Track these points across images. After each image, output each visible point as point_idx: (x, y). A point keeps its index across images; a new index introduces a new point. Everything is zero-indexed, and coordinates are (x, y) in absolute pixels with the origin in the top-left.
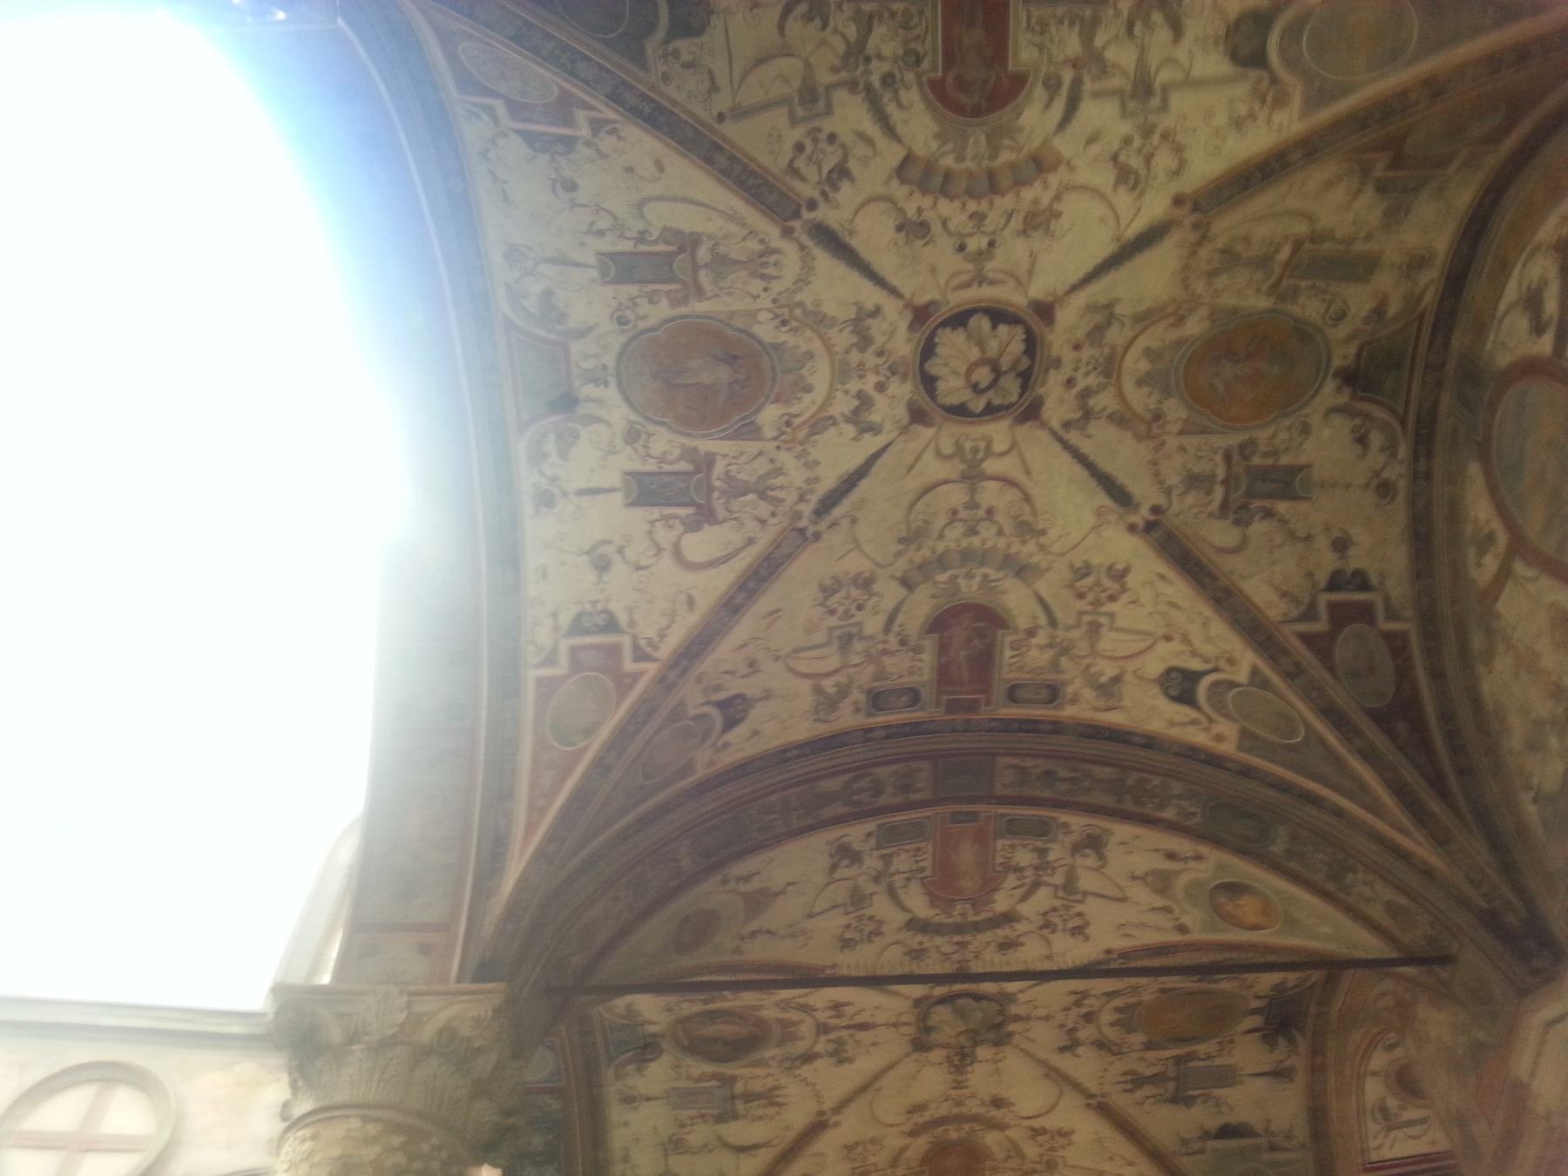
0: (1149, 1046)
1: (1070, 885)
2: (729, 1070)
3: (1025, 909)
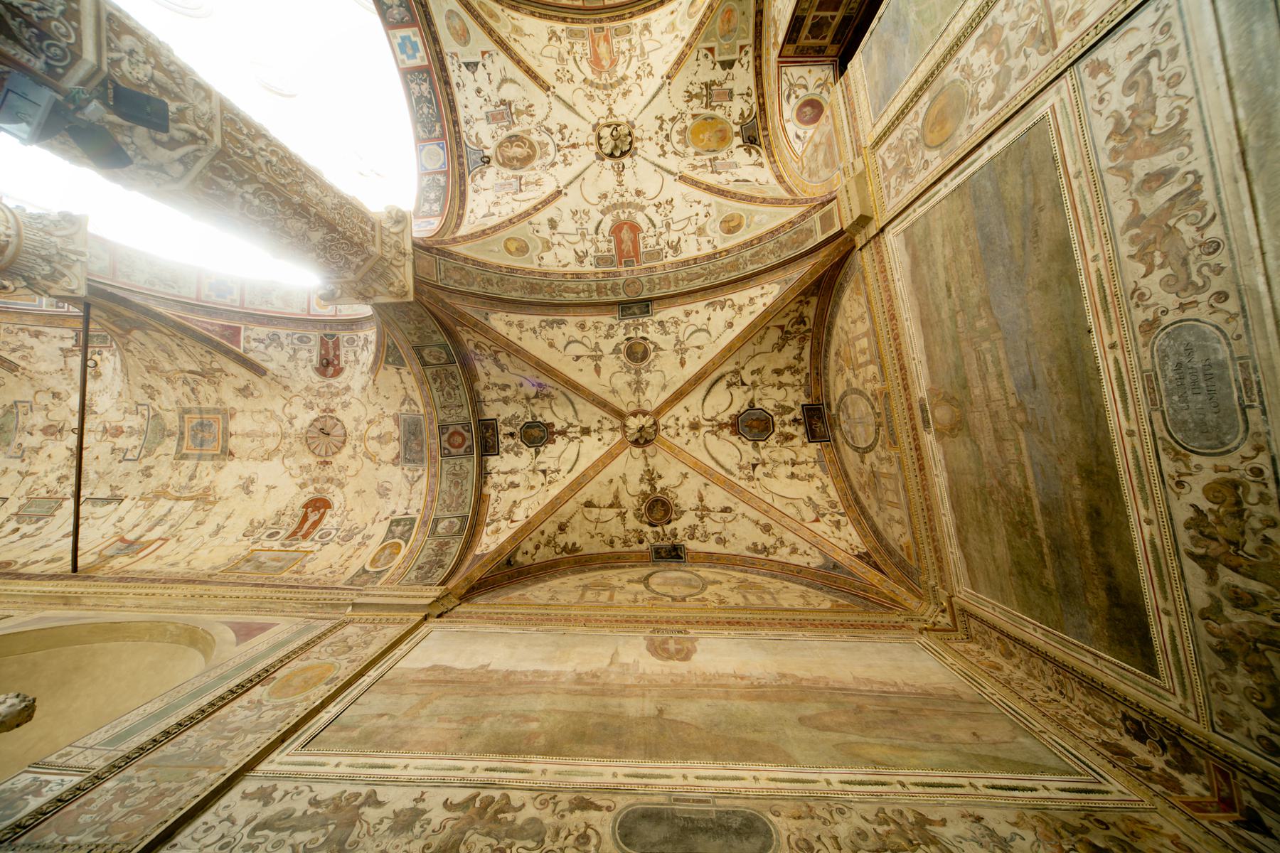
0: (697, 154)
1: (643, 53)
2: (519, 173)
3: (631, 73)
